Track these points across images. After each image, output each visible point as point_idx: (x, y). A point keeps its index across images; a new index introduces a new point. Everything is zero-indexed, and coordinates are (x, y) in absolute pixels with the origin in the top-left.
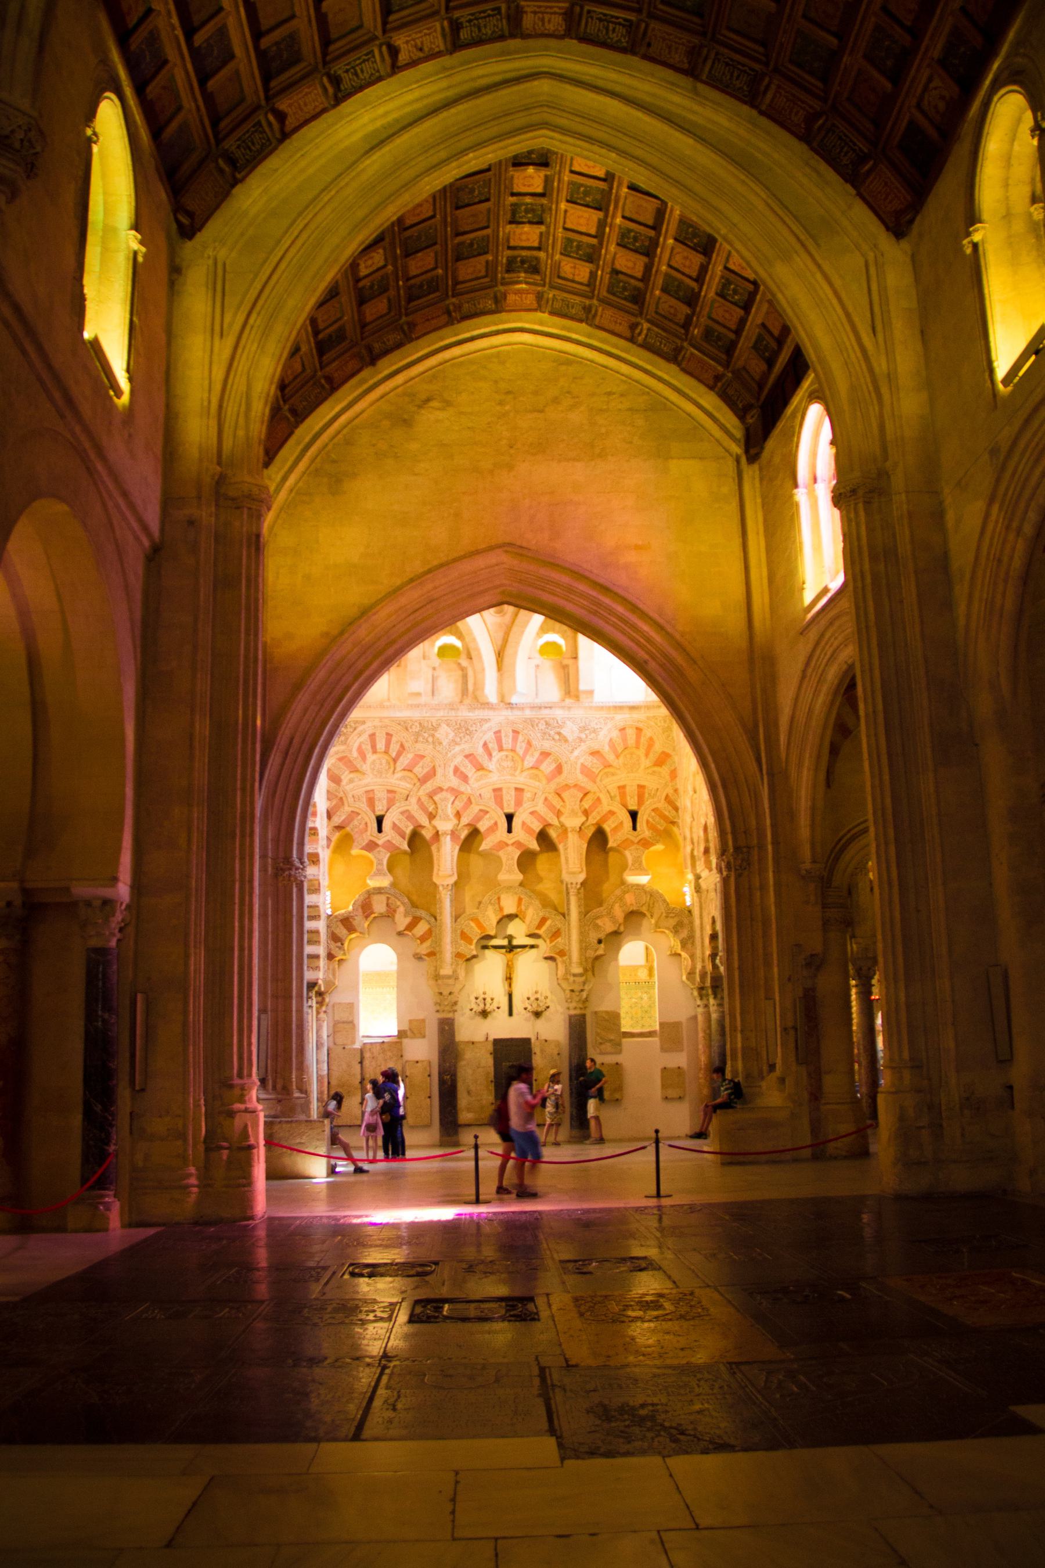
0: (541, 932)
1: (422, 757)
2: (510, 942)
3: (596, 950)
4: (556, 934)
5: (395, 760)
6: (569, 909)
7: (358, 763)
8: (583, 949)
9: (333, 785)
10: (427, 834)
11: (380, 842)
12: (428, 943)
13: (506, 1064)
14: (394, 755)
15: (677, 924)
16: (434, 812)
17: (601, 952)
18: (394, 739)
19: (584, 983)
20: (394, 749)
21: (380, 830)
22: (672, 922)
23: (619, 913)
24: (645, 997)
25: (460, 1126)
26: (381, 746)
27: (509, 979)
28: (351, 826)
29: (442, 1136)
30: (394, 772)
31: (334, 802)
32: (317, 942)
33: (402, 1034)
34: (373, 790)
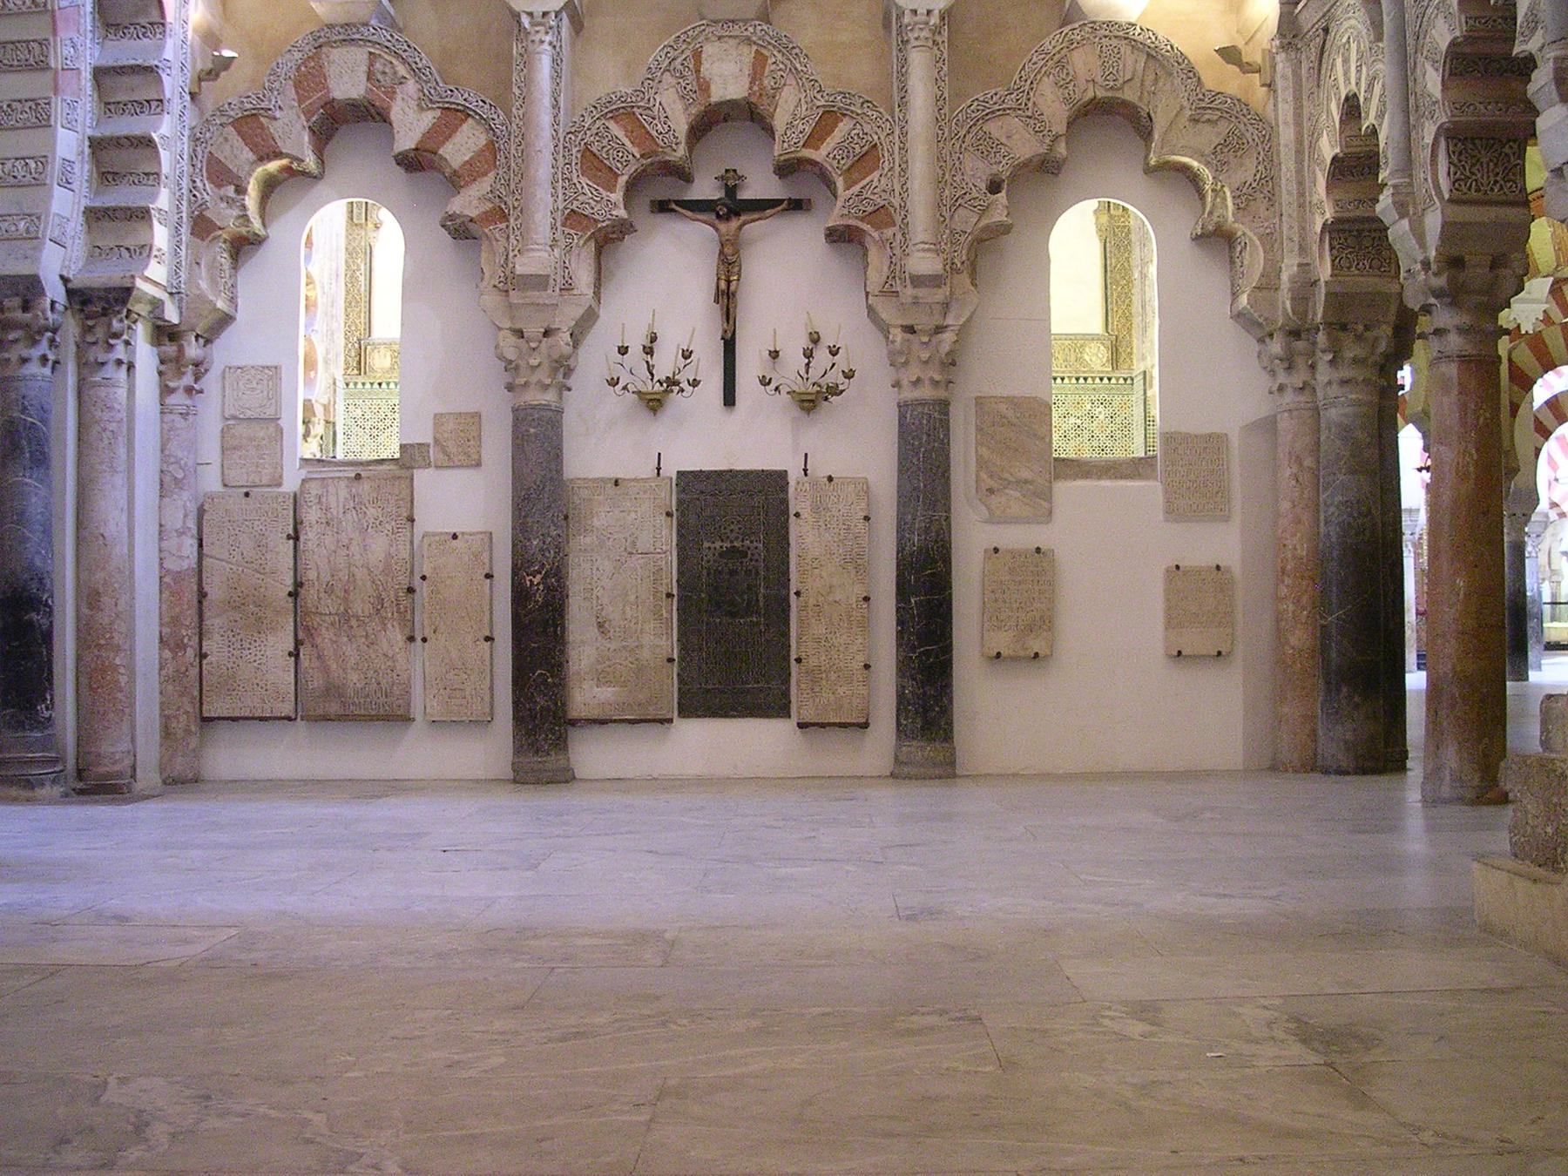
0: (819, 155)
2: (731, 191)
3: (984, 211)
4: (865, 160)
6: (903, 89)
8: (947, 203)
12: (484, 185)
13: (712, 546)
15: (1225, 144)
17: (998, 215)
19: (946, 306)
22: (1209, 137)
23: (1053, 106)
24: (1101, 413)
25: (573, 723)
27: (726, 298)
29: (518, 751)
33: (410, 457)
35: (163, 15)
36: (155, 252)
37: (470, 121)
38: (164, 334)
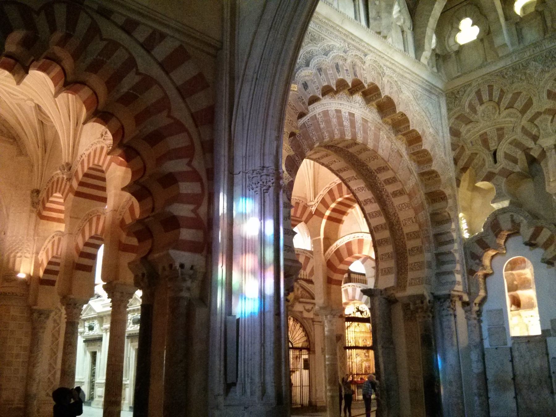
1: (519, 94)
5: (498, 104)
7: (473, 117)
9: (455, 138)
10: (535, 154)
11: (496, 171)
14: (497, 100)
16: (537, 134)
18: (495, 87)
20: (496, 94)
21: (495, 162)
26: (485, 97)
28: (472, 165)
30: (499, 114)
31: (458, 151)
32: (453, 261)
34: (486, 133)
35: (450, 216)
36: (456, 283)
37: (544, 229)
38: (465, 304)
